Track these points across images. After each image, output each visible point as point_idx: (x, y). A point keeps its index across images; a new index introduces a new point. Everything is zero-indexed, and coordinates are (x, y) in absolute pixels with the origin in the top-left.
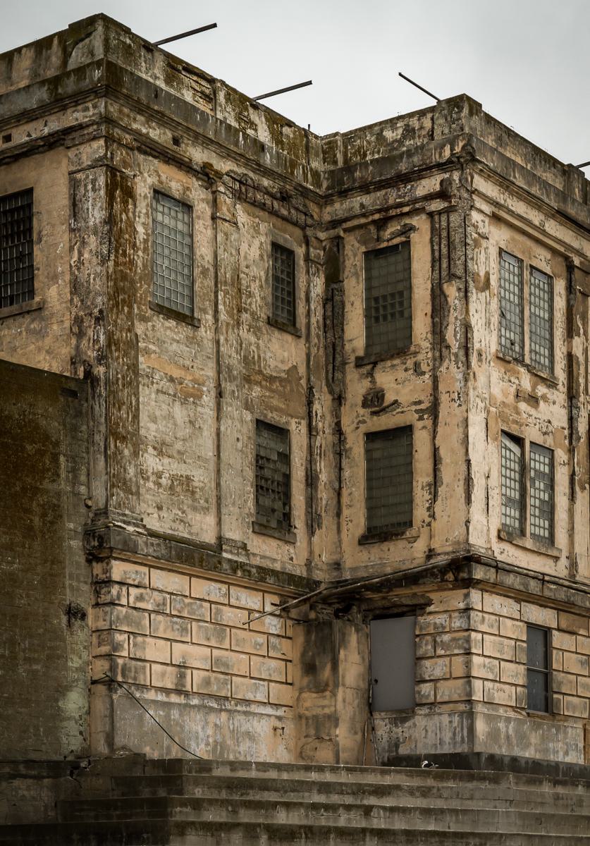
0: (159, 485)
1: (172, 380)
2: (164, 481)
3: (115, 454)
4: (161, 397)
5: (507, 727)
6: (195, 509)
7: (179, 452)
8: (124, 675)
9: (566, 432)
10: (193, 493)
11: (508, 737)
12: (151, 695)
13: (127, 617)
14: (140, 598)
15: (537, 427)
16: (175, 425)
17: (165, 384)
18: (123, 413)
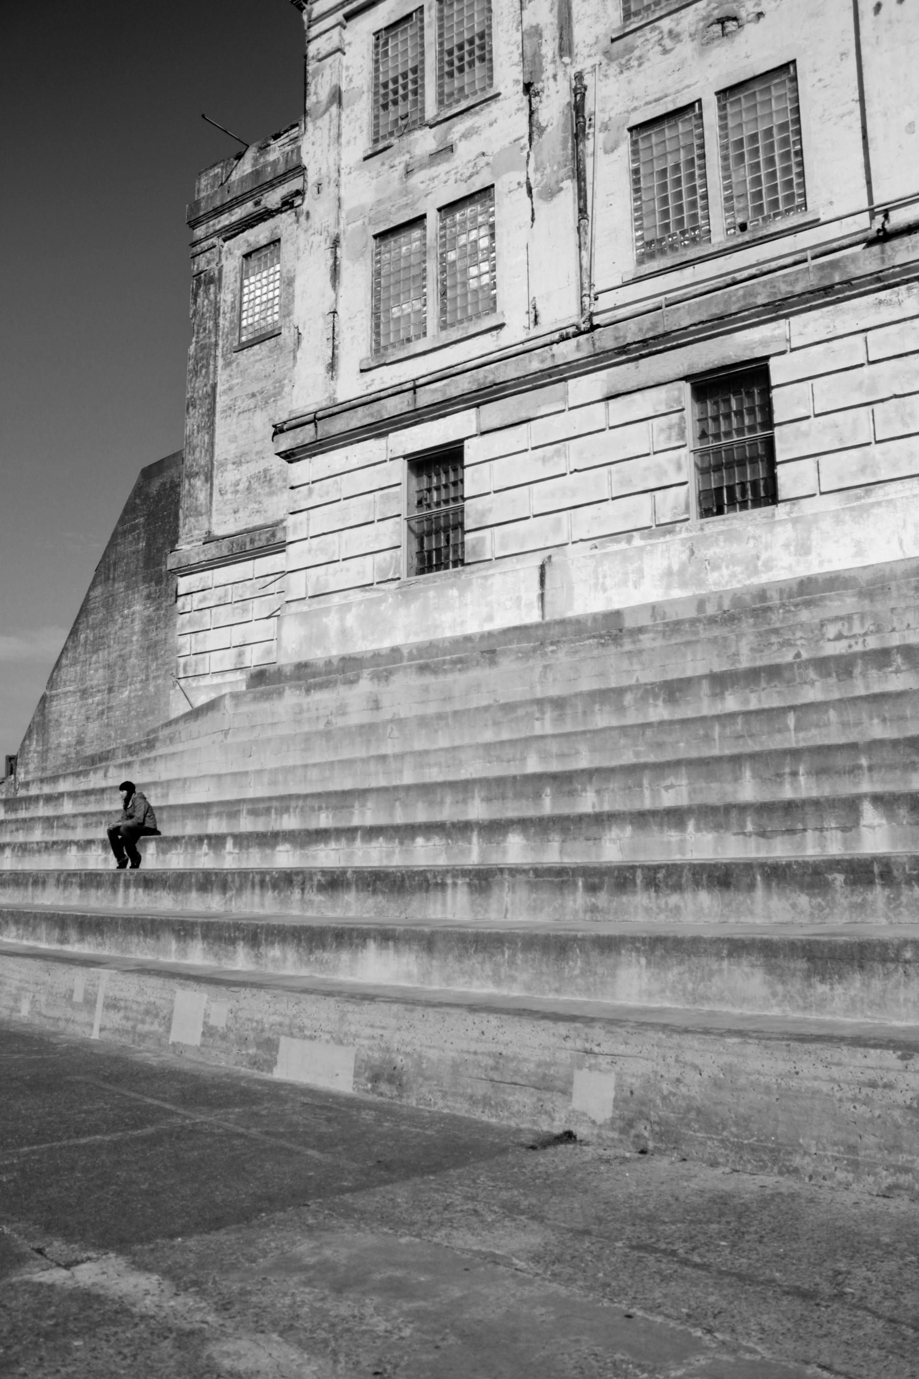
0: (237, 492)
1: (253, 395)
2: (242, 487)
3: (189, 491)
4: (242, 416)
5: (342, 619)
6: (271, 494)
7: (257, 453)
8: (185, 671)
9: (525, 140)
10: (271, 480)
11: (344, 633)
12: (206, 681)
13: (189, 621)
14: (204, 599)
15: (452, 181)
16: (255, 431)
17: (251, 403)
18: (197, 454)
